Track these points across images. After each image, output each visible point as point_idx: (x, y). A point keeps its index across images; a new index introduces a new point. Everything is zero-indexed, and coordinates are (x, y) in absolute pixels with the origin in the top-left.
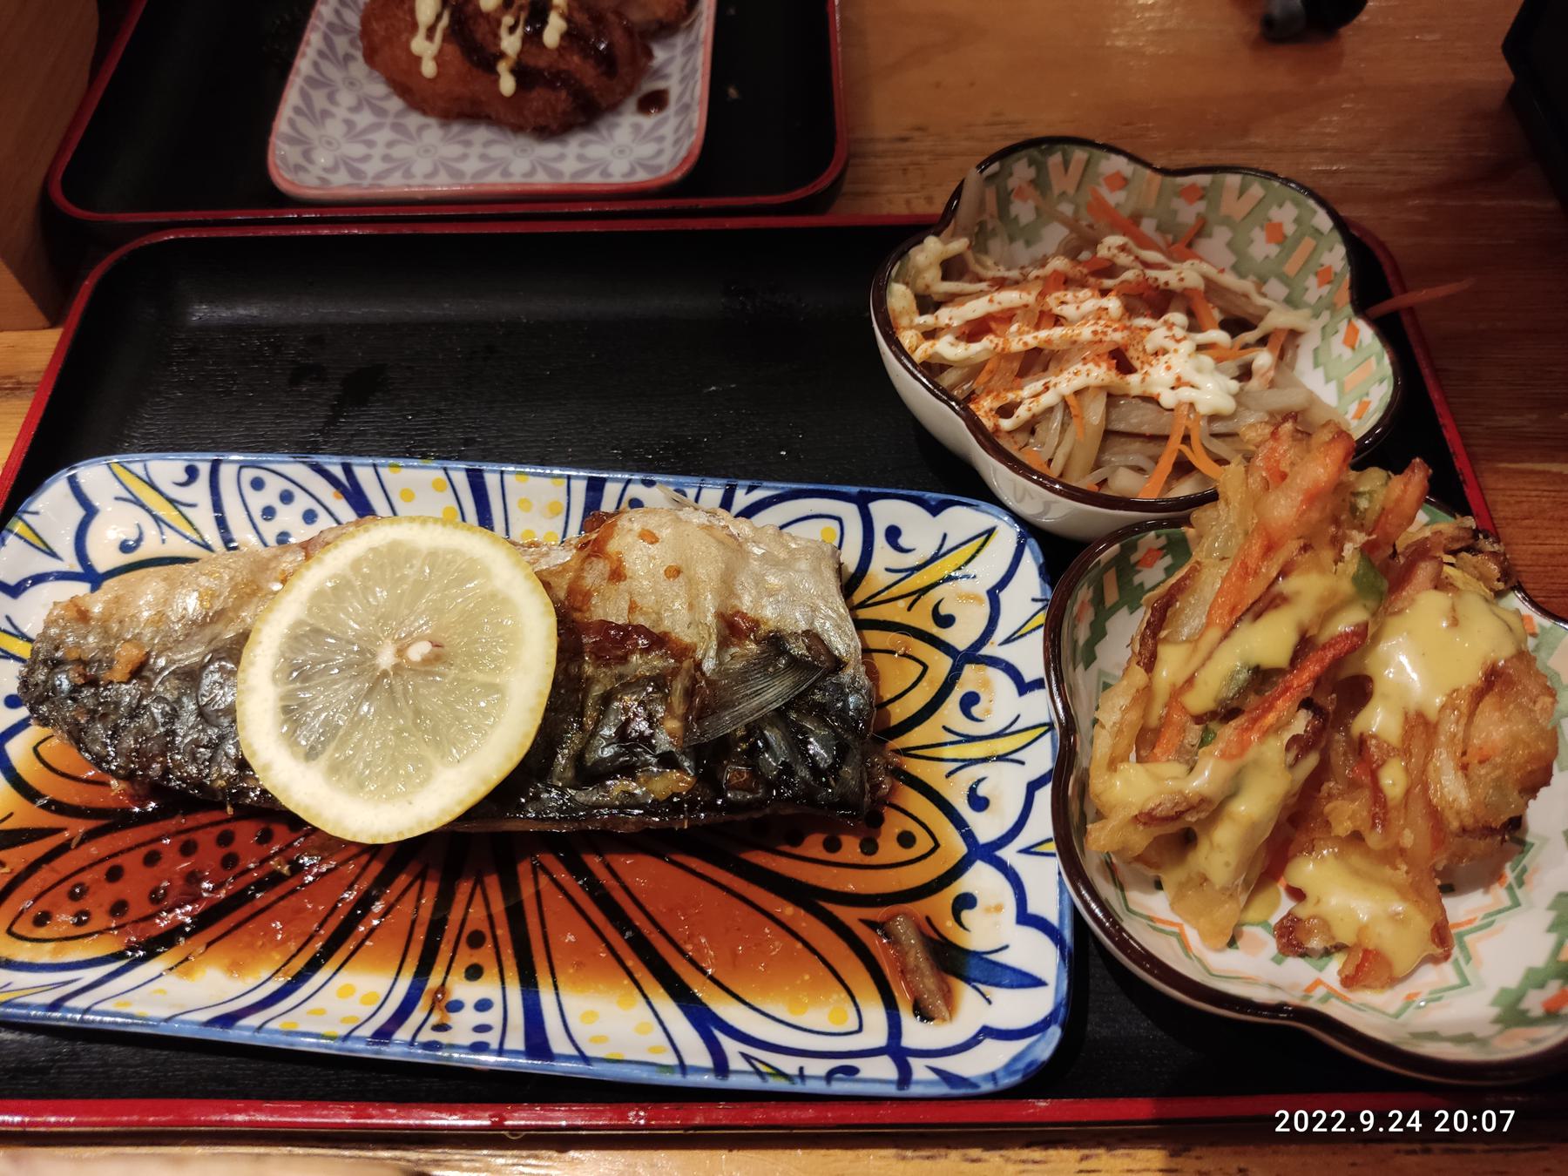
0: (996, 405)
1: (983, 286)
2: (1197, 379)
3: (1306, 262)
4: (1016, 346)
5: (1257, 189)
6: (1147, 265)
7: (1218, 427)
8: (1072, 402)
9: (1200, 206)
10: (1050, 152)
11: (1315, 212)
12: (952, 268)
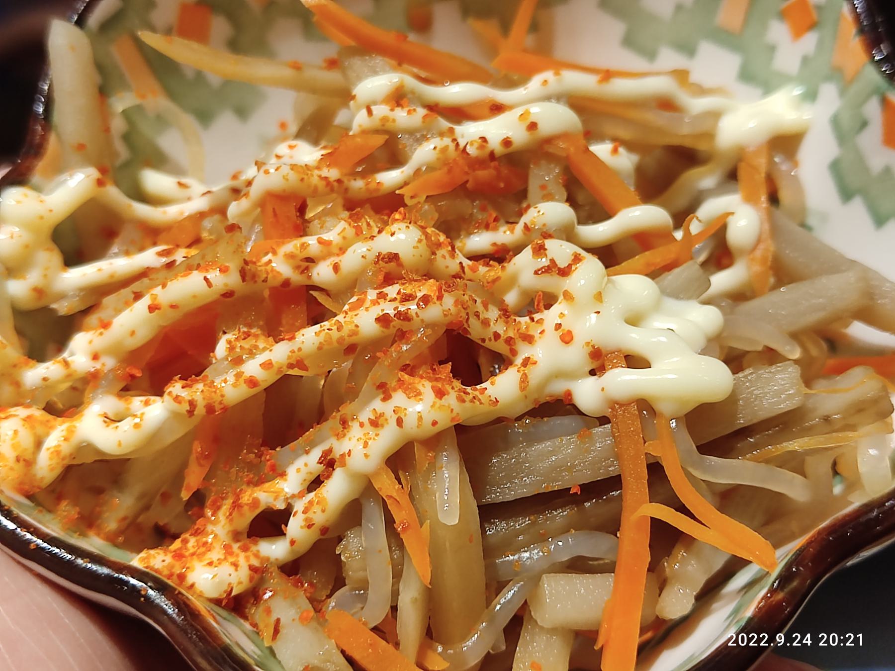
6: (459, 114)
8: (387, 485)
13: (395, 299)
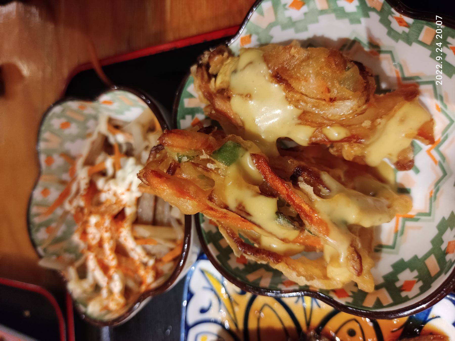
2: (127, 182)
5: (45, 135)
11: (54, 113)
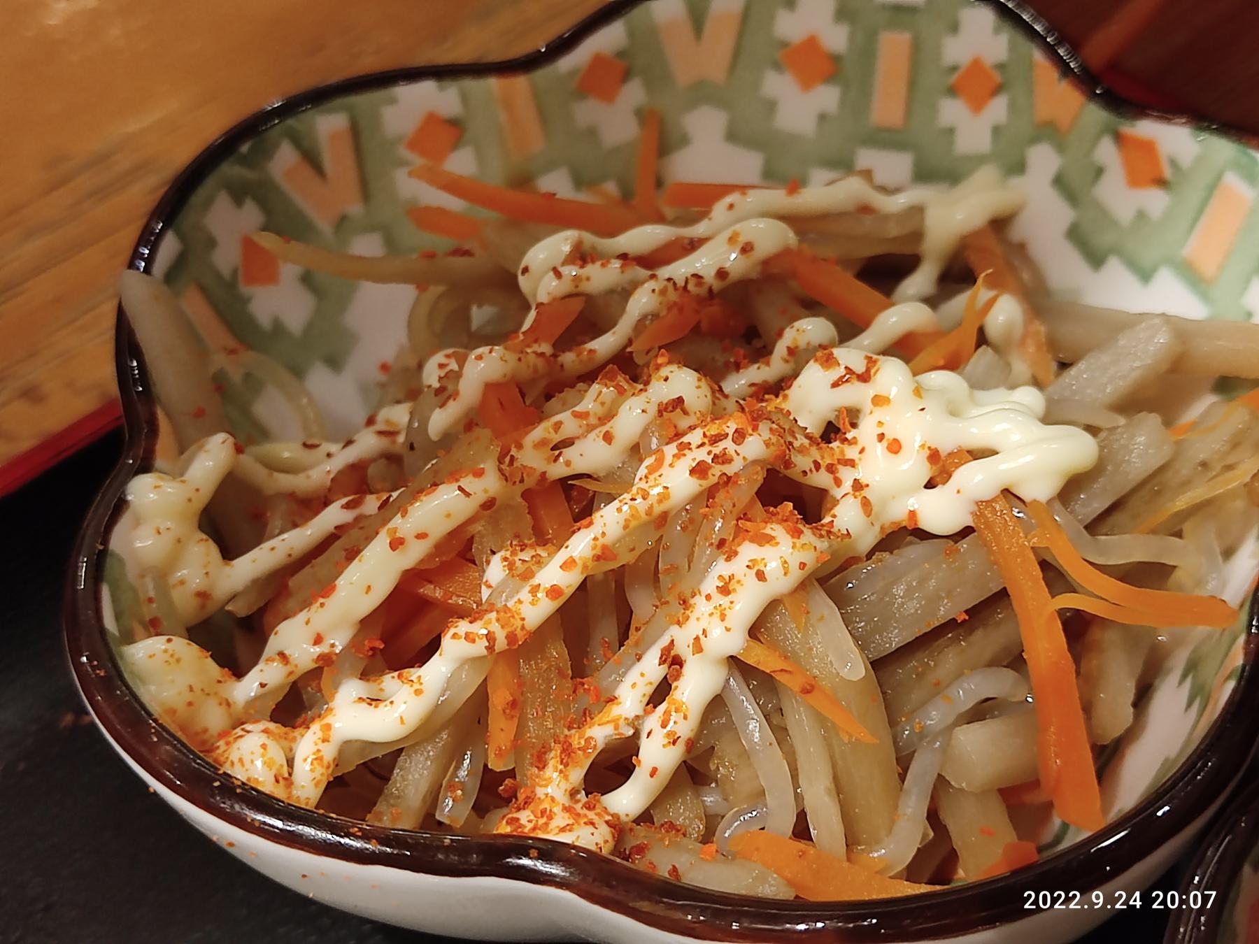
0: (577, 775)
1: (334, 515)
2: (974, 432)
3: (912, 84)
4: (534, 610)
6: (651, 261)
7: (1092, 503)
8: (761, 658)
9: (633, 93)
10: (264, 153)
12: (230, 520)
13: (703, 445)
